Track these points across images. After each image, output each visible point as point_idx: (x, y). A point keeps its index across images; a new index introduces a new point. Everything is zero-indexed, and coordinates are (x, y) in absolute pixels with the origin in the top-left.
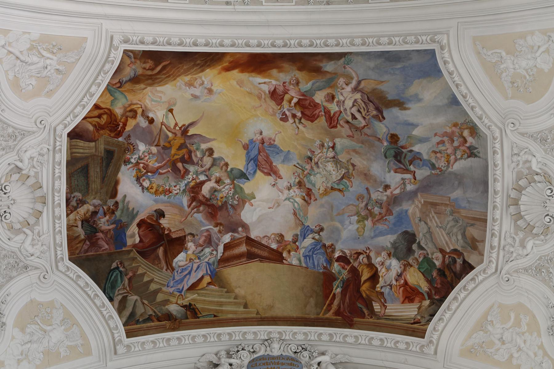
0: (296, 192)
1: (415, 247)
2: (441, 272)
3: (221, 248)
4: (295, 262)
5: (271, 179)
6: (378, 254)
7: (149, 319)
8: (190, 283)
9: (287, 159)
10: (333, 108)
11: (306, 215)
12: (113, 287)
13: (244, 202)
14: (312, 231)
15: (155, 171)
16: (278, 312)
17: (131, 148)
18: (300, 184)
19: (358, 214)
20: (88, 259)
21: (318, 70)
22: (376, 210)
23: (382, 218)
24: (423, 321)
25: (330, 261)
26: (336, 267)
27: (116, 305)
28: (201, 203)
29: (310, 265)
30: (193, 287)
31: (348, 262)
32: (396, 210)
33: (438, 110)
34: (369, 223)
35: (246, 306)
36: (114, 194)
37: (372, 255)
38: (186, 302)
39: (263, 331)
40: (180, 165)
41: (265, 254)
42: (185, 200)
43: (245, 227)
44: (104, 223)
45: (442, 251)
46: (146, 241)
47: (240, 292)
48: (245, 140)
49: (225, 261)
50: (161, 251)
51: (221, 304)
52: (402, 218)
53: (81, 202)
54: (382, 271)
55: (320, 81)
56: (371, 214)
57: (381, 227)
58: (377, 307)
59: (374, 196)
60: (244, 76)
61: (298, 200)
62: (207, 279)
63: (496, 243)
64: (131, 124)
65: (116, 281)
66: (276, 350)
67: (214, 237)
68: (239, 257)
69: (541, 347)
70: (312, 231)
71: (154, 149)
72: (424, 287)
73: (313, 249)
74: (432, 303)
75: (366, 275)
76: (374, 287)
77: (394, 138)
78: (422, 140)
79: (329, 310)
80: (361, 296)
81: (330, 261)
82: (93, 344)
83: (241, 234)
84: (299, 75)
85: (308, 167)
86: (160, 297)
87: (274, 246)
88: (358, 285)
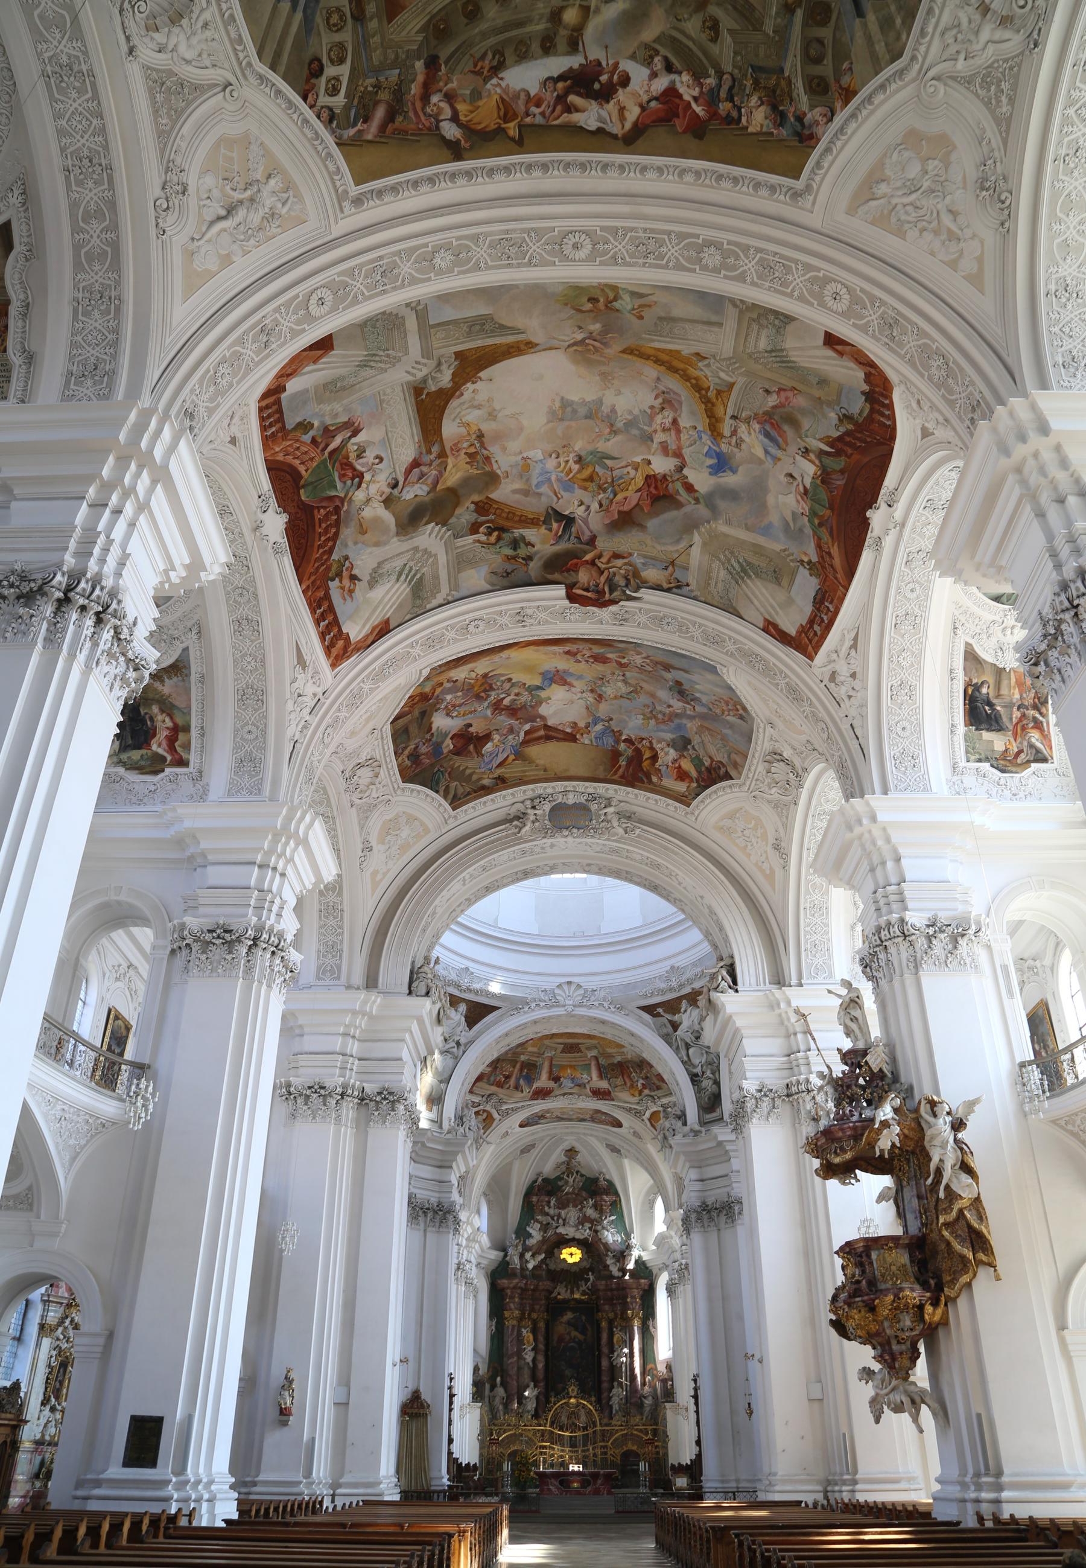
0: (590, 698)
1: (689, 747)
2: (708, 770)
3: (522, 735)
4: (587, 742)
5: (566, 688)
6: (659, 742)
7: (469, 794)
8: (498, 762)
9: (580, 677)
10: (623, 661)
11: (597, 709)
12: (437, 783)
13: (541, 703)
14: (603, 720)
15: (460, 705)
16: (572, 773)
17: (439, 700)
18: (592, 691)
19: (643, 714)
20: (416, 775)
21: (610, 646)
22: (660, 716)
23: (664, 722)
24: (690, 797)
25: (617, 741)
26: (622, 746)
27: (442, 792)
28: (503, 710)
29: (600, 743)
30: (500, 765)
31: (633, 744)
32: (677, 721)
33: (717, 686)
34: (652, 722)
35: (545, 770)
36: (430, 729)
37: (654, 742)
38: (496, 775)
39: (560, 786)
40: (483, 694)
41: (561, 736)
42: (489, 712)
43: (543, 718)
44: (424, 749)
45: (710, 758)
46: (459, 745)
47: (541, 762)
48: (542, 670)
49: (526, 743)
50: (471, 747)
51: (524, 771)
52: (680, 727)
53: (406, 748)
54: (661, 754)
55: (611, 649)
56: (655, 717)
57: (663, 727)
58: (654, 779)
59: (658, 708)
60: (541, 648)
61: (591, 699)
62: (512, 757)
63: (751, 776)
64: (438, 691)
65: (439, 778)
66: (571, 800)
67: (516, 728)
68: (539, 738)
69: (766, 852)
70: (603, 720)
71: (460, 694)
72: (694, 774)
73: (603, 733)
74: (699, 786)
75: (647, 754)
76: (654, 764)
77: (678, 683)
78: (701, 692)
79: (616, 773)
80: (642, 770)
81: (617, 741)
82: (430, 826)
83: (539, 722)
84: (593, 647)
85: (600, 682)
86: (475, 777)
87: (569, 730)
88: (640, 760)
